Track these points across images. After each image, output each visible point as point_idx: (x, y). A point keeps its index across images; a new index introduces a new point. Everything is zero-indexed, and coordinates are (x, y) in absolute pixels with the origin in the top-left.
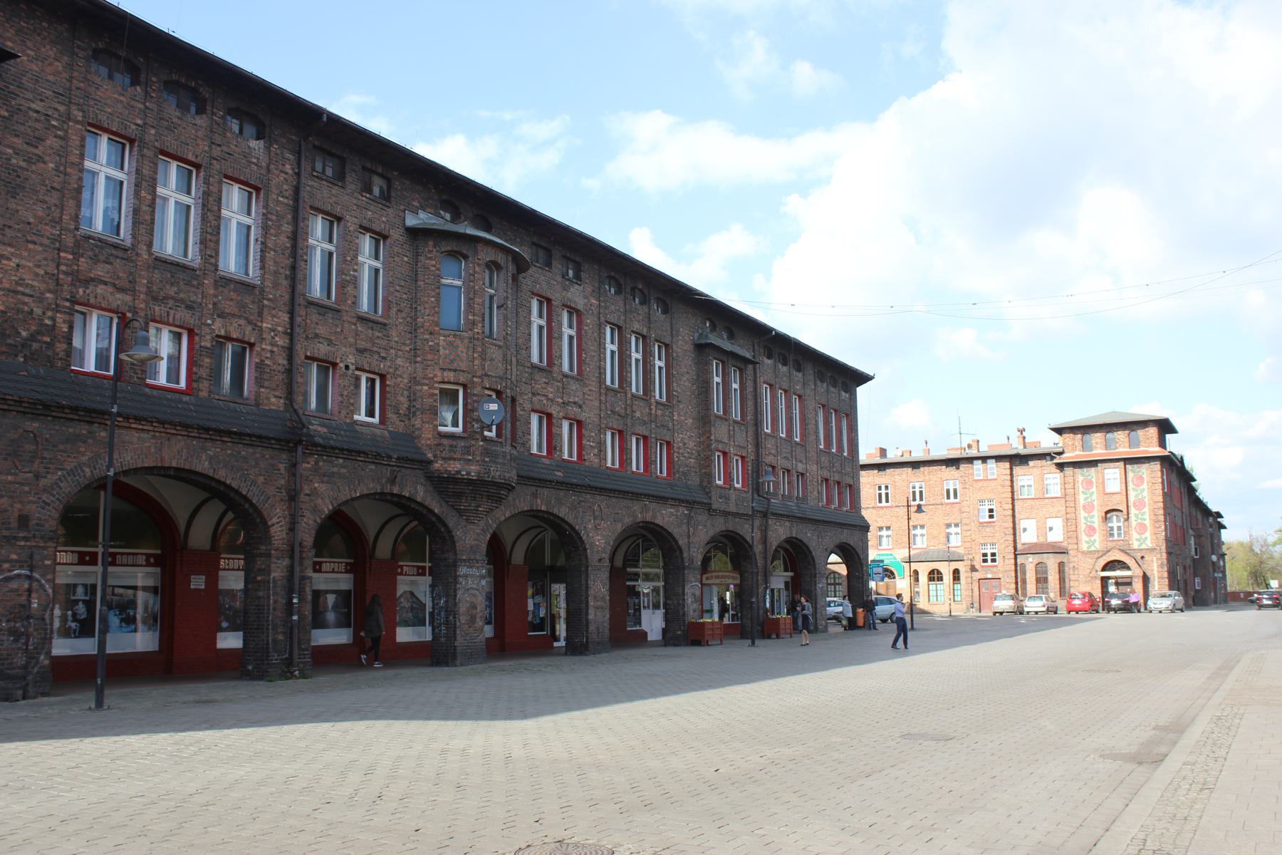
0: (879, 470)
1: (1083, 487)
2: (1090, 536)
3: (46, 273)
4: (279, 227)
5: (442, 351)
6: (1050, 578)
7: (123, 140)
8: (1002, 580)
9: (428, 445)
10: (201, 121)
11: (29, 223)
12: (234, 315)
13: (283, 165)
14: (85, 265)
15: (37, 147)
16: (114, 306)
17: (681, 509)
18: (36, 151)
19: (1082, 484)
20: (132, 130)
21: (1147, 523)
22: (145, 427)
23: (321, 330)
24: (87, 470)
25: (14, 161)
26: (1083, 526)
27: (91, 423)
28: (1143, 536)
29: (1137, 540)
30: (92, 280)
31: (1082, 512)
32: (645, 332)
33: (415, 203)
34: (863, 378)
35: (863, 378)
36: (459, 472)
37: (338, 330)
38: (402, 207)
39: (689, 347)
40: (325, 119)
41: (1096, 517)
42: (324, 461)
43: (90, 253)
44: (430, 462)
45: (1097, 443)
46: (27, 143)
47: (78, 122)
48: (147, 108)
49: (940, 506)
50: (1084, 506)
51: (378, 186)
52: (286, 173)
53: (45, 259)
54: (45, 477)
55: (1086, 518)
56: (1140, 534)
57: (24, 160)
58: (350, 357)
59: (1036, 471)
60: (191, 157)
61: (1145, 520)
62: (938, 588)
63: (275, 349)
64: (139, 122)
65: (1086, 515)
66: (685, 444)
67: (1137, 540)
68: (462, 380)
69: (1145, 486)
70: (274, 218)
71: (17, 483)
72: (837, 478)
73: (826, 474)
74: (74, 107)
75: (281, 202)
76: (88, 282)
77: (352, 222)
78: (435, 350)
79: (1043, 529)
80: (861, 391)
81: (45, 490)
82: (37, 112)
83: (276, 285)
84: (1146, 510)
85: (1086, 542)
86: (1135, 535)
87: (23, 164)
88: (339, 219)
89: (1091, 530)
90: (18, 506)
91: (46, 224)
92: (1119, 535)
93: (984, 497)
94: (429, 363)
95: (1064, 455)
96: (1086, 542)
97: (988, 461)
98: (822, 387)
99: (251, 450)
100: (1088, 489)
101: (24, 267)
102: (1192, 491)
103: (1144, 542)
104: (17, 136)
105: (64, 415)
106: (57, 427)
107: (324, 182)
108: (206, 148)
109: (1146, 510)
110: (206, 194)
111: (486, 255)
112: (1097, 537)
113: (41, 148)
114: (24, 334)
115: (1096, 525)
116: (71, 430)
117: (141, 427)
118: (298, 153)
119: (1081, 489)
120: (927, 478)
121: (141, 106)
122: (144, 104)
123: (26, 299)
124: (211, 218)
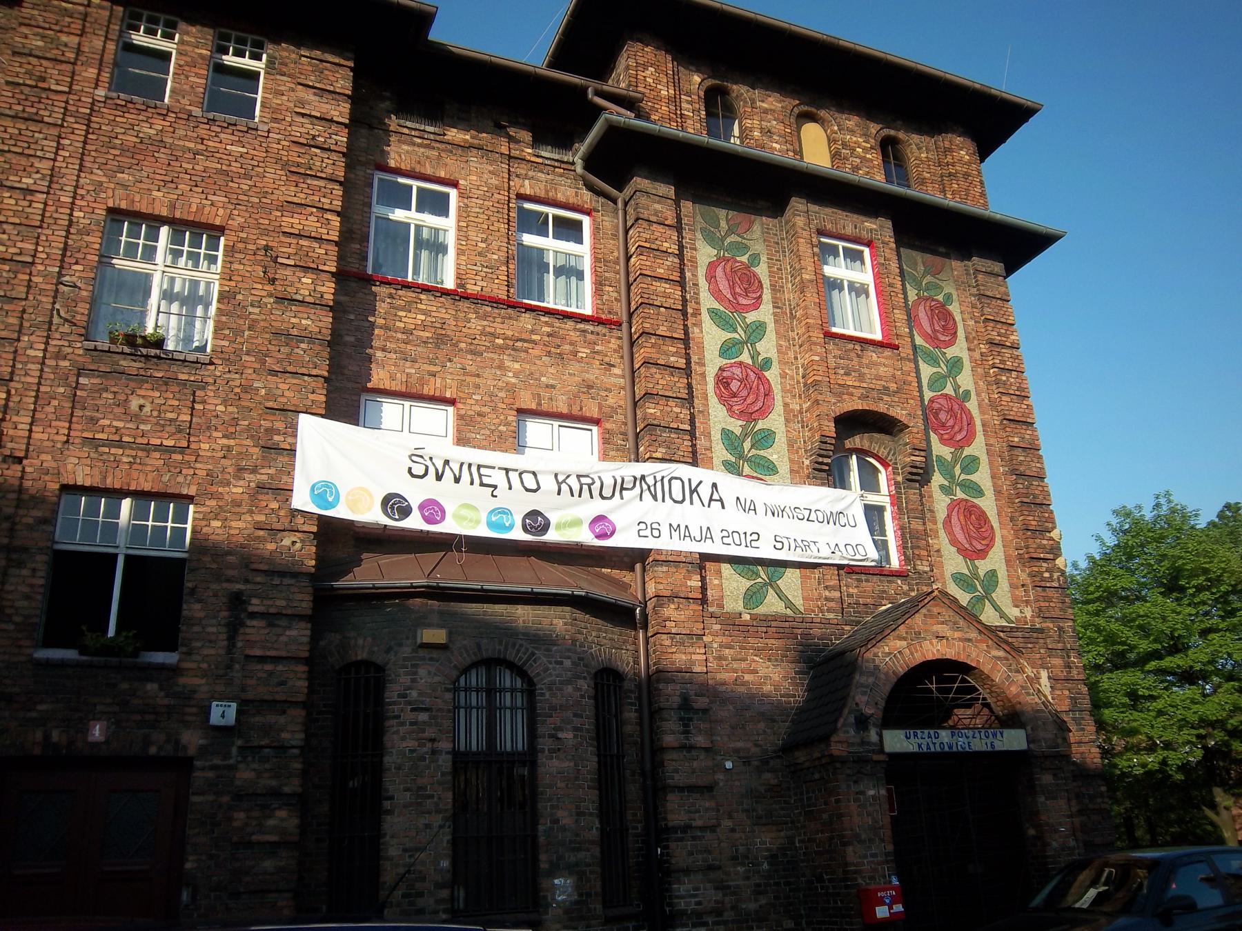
1: (716, 294)
8: (201, 776)
19: (711, 277)
28: (983, 566)
41: (781, 439)
50: (723, 381)
61: (980, 493)
65: (736, 426)
84: (977, 448)
100: (741, 309)
103: (987, 596)
119: (707, 301)
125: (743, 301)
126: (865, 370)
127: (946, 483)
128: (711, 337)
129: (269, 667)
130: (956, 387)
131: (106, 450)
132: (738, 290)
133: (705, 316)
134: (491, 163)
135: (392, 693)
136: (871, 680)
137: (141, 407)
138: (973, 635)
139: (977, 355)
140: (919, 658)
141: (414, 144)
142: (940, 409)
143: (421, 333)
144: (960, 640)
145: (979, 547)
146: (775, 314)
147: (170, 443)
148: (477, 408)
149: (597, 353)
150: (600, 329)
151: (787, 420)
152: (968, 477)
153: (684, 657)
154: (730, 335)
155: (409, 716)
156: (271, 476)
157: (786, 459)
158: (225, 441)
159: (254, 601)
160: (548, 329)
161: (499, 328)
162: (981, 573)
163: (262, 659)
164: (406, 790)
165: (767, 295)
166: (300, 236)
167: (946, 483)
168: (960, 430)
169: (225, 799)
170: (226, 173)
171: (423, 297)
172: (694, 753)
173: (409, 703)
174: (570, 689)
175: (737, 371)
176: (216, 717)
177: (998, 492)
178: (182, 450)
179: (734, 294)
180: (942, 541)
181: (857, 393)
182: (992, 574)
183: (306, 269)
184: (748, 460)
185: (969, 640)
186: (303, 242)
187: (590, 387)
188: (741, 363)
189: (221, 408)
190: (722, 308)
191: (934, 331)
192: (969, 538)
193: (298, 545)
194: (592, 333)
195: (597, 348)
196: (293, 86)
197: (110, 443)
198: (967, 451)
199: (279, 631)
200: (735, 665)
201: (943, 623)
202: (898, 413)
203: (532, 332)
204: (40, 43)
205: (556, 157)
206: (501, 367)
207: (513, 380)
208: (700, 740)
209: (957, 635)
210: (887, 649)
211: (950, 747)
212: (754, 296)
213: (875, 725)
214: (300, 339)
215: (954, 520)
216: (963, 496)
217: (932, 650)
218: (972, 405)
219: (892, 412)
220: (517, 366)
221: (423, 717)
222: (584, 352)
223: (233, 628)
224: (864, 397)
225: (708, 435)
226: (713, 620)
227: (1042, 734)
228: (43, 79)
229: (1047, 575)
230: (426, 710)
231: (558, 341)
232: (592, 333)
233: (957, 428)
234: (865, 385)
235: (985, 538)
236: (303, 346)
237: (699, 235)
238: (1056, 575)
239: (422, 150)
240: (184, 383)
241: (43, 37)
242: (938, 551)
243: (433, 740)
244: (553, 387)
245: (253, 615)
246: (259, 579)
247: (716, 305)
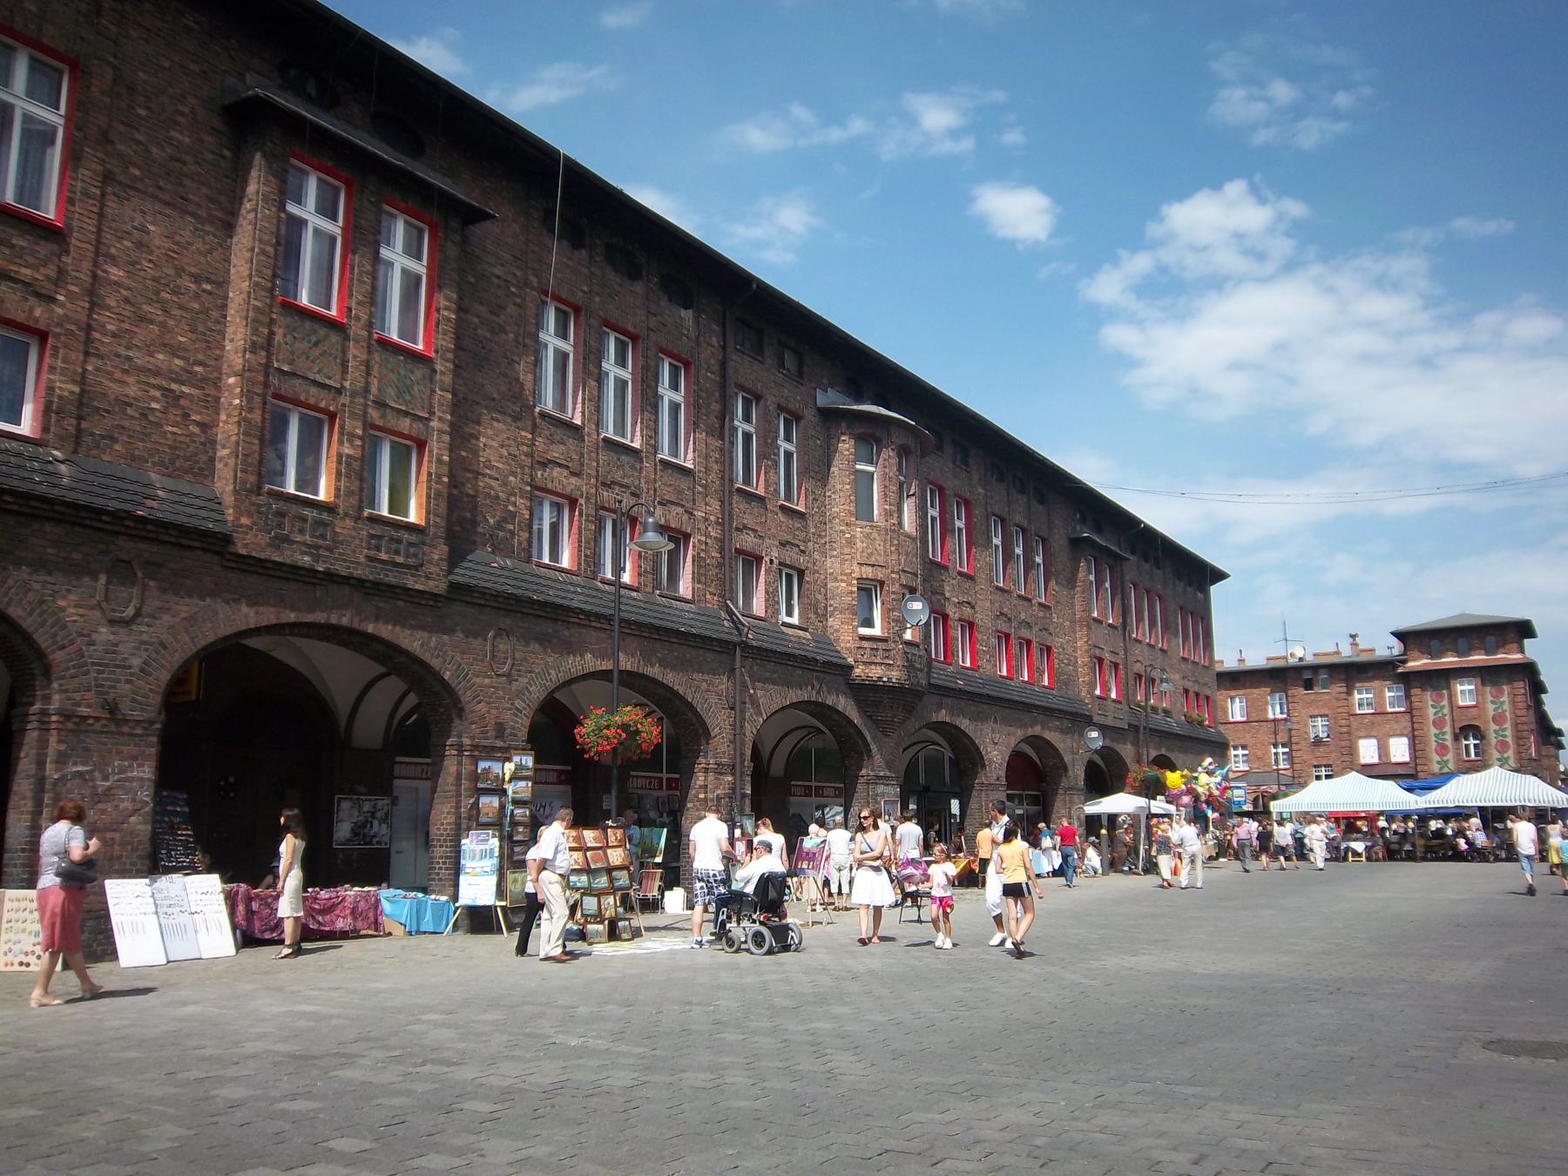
3: (510, 454)
4: (708, 405)
5: (859, 544)
7: (570, 310)
9: (847, 649)
10: (639, 287)
11: (494, 399)
12: (672, 503)
13: (710, 337)
14: (543, 445)
15: (498, 316)
16: (568, 491)
17: (1065, 721)
18: (498, 320)
20: (579, 299)
21: (1509, 740)
22: (603, 626)
23: (749, 520)
24: (553, 673)
25: (480, 331)
27: (555, 620)
30: (550, 462)
32: (1026, 525)
33: (825, 381)
34: (1219, 576)
35: (1219, 576)
36: (880, 678)
37: (763, 520)
38: (813, 385)
39: (1064, 541)
40: (755, 286)
42: (757, 664)
43: (547, 433)
44: (851, 668)
46: (491, 312)
47: (533, 289)
48: (591, 272)
51: (790, 361)
52: (713, 346)
53: (508, 439)
54: (517, 680)
55: (1436, 735)
57: (488, 331)
58: (774, 549)
60: (630, 328)
63: (708, 541)
64: (585, 288)
65: (1437, 732)
66: (1064, 649)
68: (880, 576)
69: (1505, 698)
70: (704, 395)
71: (493, 687)
72: (1196, 688)
73: (1189, 685)
74: (530, 272)
75: (710, 378)
76: (545, 464)
77: (771, 401)
78: (851, 542)
79: (1383, 750)
80: (1215, 590)
81: (518, 697)
82: (498, 277)
83: (707, 470)
85: (1438, 763)
87: (488, 335)
88: (758, 398)
89: (1442, 749)
90: (494, 712)
91: (508, 400)
92: (1476, 754)
93: (1316, 712)
94: (847, 557)
95: (1410, 664)
96: (1438, 763)
97: (1321, 671)
98: (1180, 586)
99: (694, 653)
100: (1438, 702)
101: (491, 447)
102: (1538, 704)
104: (481, 303)
105: (533, 612)
106: (526, 625)
107: (745, 357)
108: (643, 318)
109: (1508, 725)
110: (646, 368)
111: (898, 438)
112: (1450, 756)
113: (502, 317)
114: (491, 521)
116: (538, 628)
117: (599, 625)
118: (724, 325)
121: (586, 271)
122: (589, 268)
123: (493, 483)
124: (650, 395)
128: (1431, 711)
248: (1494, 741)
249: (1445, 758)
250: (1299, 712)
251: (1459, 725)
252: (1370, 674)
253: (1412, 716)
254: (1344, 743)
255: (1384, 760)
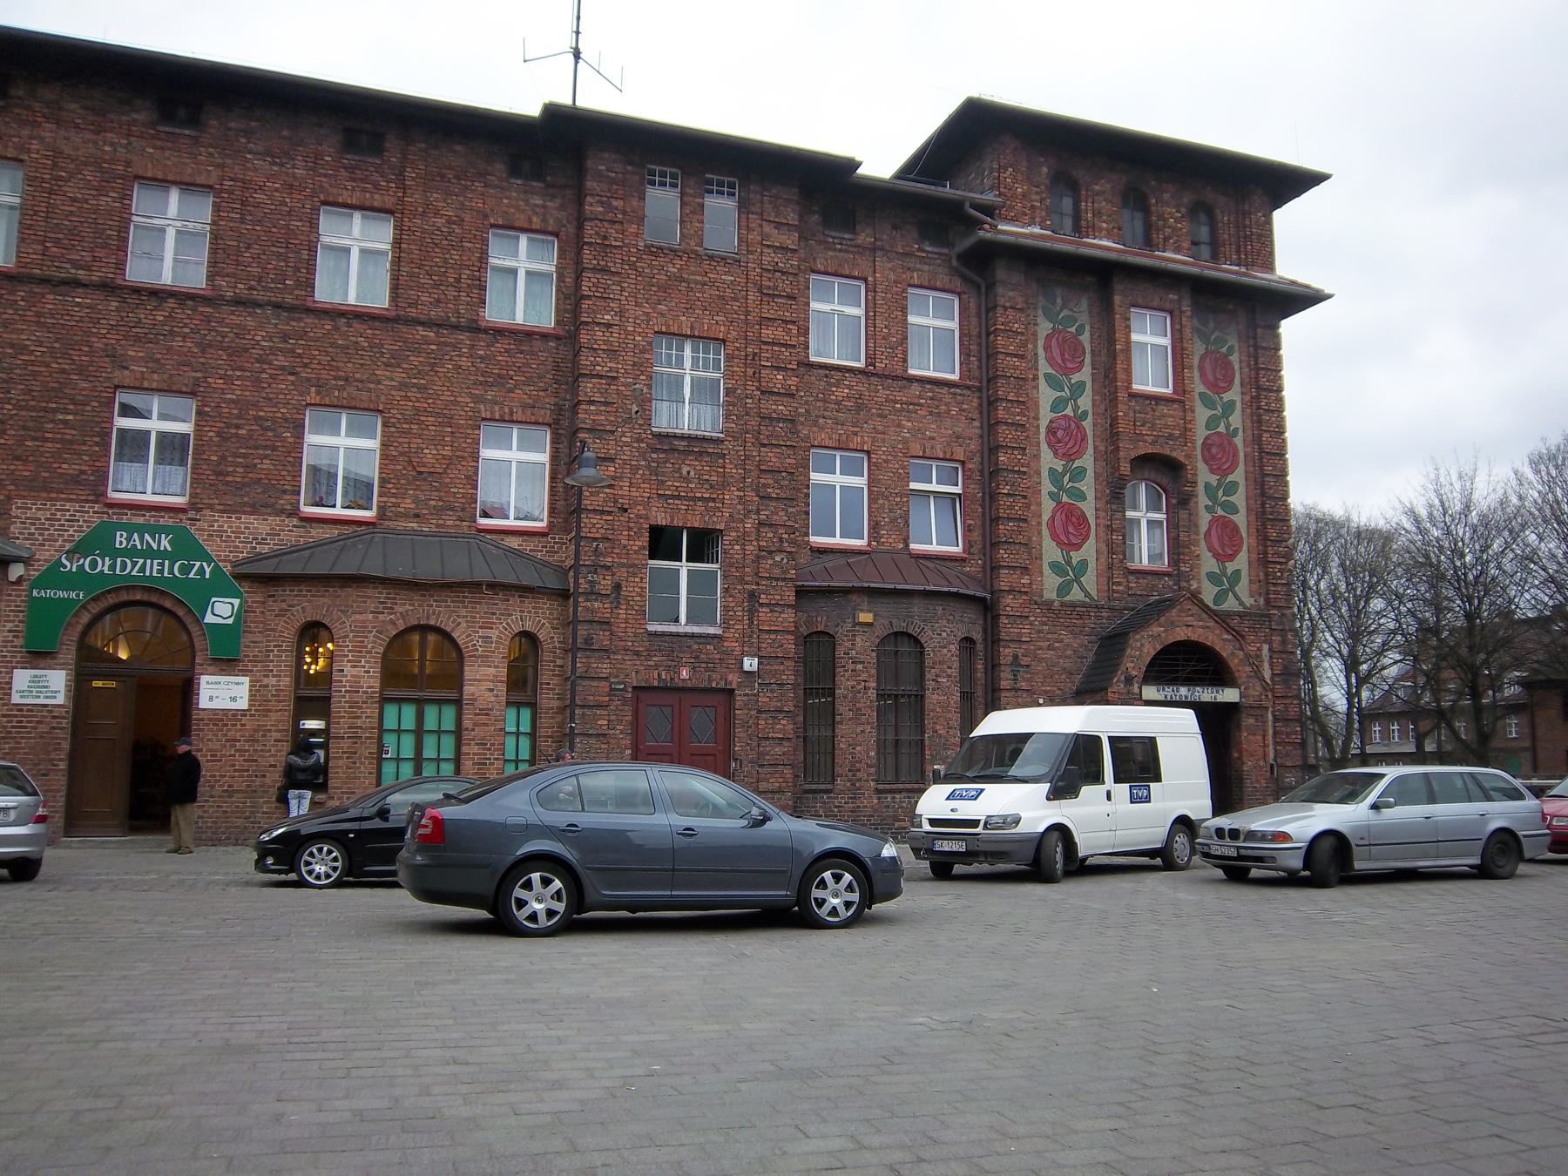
0: (167, 114)
1: (1051, 361)
2: (1069, 546)
6: (932, 698)
8: (739, 699)
19: (1047, 348)
21: (1240, 519)
26: (1048, 506)
28: (1231, 567)
29: (1213, 578)
31: (1046, 454)
41: (1090, 474)
45: (1097, 213)
49: (464, 337)
50: (1051, 431)
55: (1055, 477)
56: (1216, 555)
59: (885, 270)
62: (430, 723)
65: (1059, 465)
67: (1213, 578)
69: (1234, 394)
84: (1238, 476)
85: (1055, 567)
86: (1209, 563)
89: (1071, 526)
96: (1055, 567)
100: (1067, 372)
103: (1232, 589)
109: (1238, 476)
112: (1089, 551)
115: (1088, 507)
119: (1044, 367)
120: (415, 198)
125: (1070, 365)
126: (1158, 422)
127: (1210, 504)
128: (1046, 395)
129: (773, 636)
130: (1228, 426)
131: (672, 501)
132: (1067, 356)
133: (1042, 381)
134: (890, 260)
135: (840, 652)
136: (1138, 653)
137: (688, 473)
138: (1212, 624)
139: (1248, 398)
140: (1171, 640)
141: (835, 250)
142: (1212, 445)
143: (846, 403)
144: (1202, 627)
145: (1230, 552)
146: (1093, 374)
147: (707, 496)
148: (884, 457)
149: (964, 410)
150: (965, 392)
151: (1095, 460)
152: (1228, 498)
153: (1016, 630)
154: (1059, 394)
155: (851, 667)
156: (767, 516)
157: (1093, 489)
158: (737, 493)
159: (762, 596)
160: (930, 394)
161: (899, 396)
162: (1229, 572)
163: (769, 632)
164: (850, 710)
165: (1088, 360)
166: (773, 344)
167: (1210, 504)
168: (1226, 462)
169: (753, 712)
170: (723, 298)
171: (847, 375)
172: (1020, 693)
173: (851, 658)
174: (945, 651)
175: (1063, 422)
176: (746, 667)
177: (1249, 510)
178: (714, 500)
179: (1063, 360)
180: (1202, 550)
181: (1149, 439)
182: (1237, 573)
183: (778, 368)
184: (1067, 491)
185: (1208, 627)
186: (775, 348)
187: (958, 437)
188: (1065, 416)
189: (734, 471)
190: (1054, 372)
191: (1216, 379)
192: (1223, 546)
193: (785, 560)
194: (960, 395)
195: (964, 406)
196: (759, 222)
197: (673, 497)
198: (1230, 478)
199: (777, 614)
200: (1050, 636)
201: (1192, 616)
202: (1179, 455)
203: (920, 397)
204: (601, 209)
205: (936, 250)
206: (899, 425)
207: (907, 435)
208: (1023, 685)
209: (1201, 623)
210: (1150, 633)
211: (1186, 697)
212: (1078, 360)
213: (1137, 682)
214: (778, 420)
215: (1213, 532)
216: (1223, 513)
217: (1181, 634)
218: (1238, 441)
219: (1174, 454)
220: (910, 424)
221: (860, 667)
222: (954, 410)
223: (752, 612)
224: (1153, 443)
225: (1038, 473)
226: (1036, 606)
227: (1251, 692)
228: (605, 238)
229: (1279, 574)
230: (860, 663)
231: (936, 403)
232: (960, 395)
233: (1224, 460)
234: (1155, 433)
235: (1234, 546)
236: (781, 425)
237: (1040, 312)
238: (1285, 575)
239: (842, 254)
240: (710, 454)
241: (602, 203)
242: (1198, 556)
243: (865, 681)
244: (933, 438)
245: (761, 605)
246: (764, 583)
247: (1050, 371)
248: (1204, 519)
249: (1076, 557)
250: (621, 313)
251: (1129, 450)
252: (865, 237)
253: (992, 403)
254: (772, 458)
255: (890, 540)
